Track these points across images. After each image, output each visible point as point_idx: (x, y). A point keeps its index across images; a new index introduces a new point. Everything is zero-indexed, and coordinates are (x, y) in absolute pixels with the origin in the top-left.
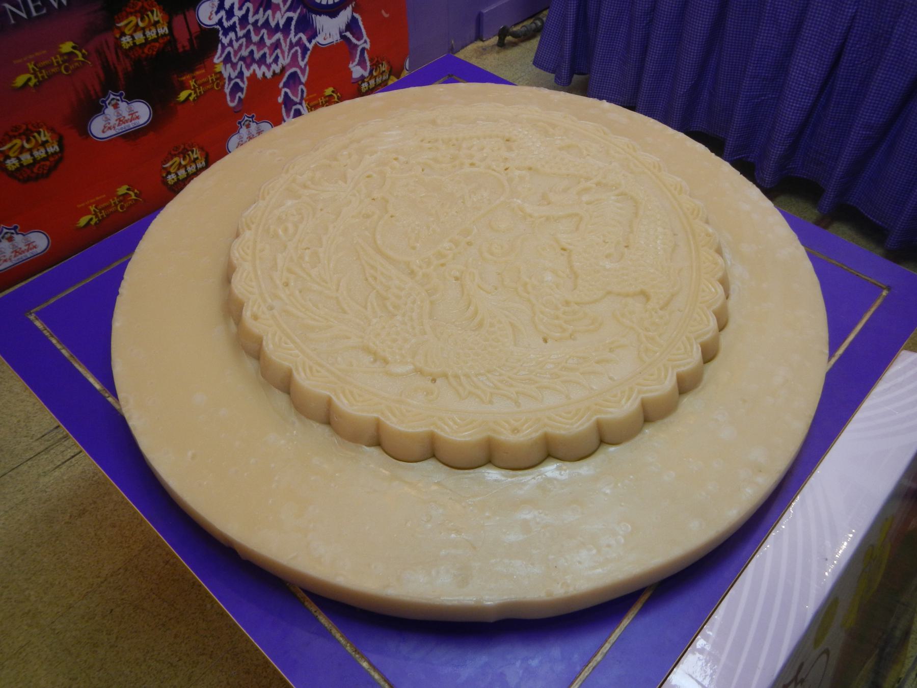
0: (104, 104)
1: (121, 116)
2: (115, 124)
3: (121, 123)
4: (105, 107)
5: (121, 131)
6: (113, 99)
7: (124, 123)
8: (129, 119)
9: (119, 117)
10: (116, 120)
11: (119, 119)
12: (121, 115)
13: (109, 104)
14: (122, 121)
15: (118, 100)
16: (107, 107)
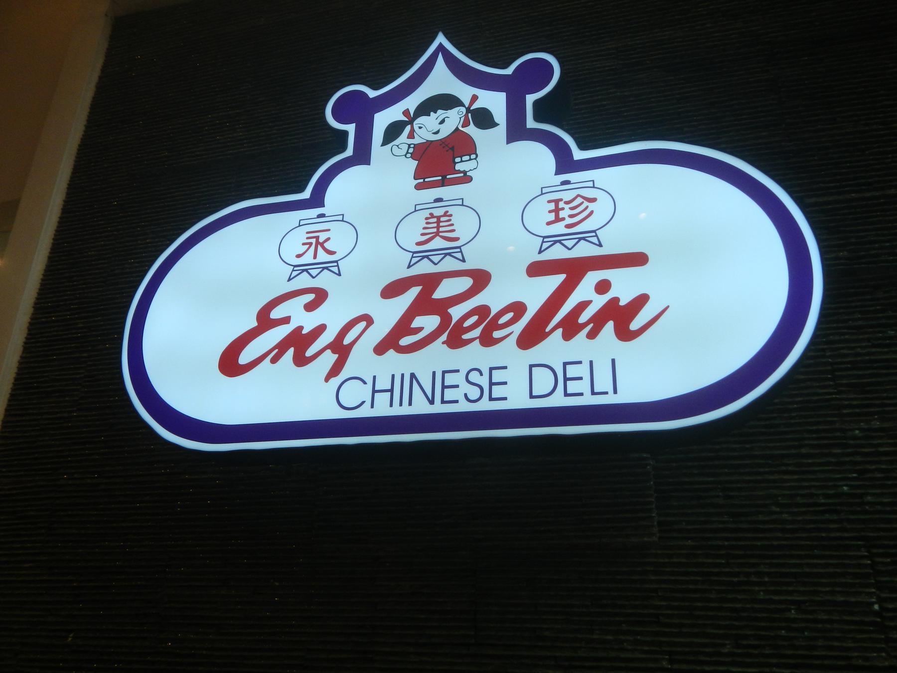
0: (351, 128)
1: (449, 264)
2: (368, 320)
3: (428, 323)
4: (349, 152)
5: (382, 408)
6: (446, 102)
7: (456, 341)
8: (518, 309)
9: (424, 268)
10: (392, 290)
11: (430, 282)
12: (454, 251)
13: (393, 132)
14: (442, 308)
15: (483, 119)
16: (362, 156)
